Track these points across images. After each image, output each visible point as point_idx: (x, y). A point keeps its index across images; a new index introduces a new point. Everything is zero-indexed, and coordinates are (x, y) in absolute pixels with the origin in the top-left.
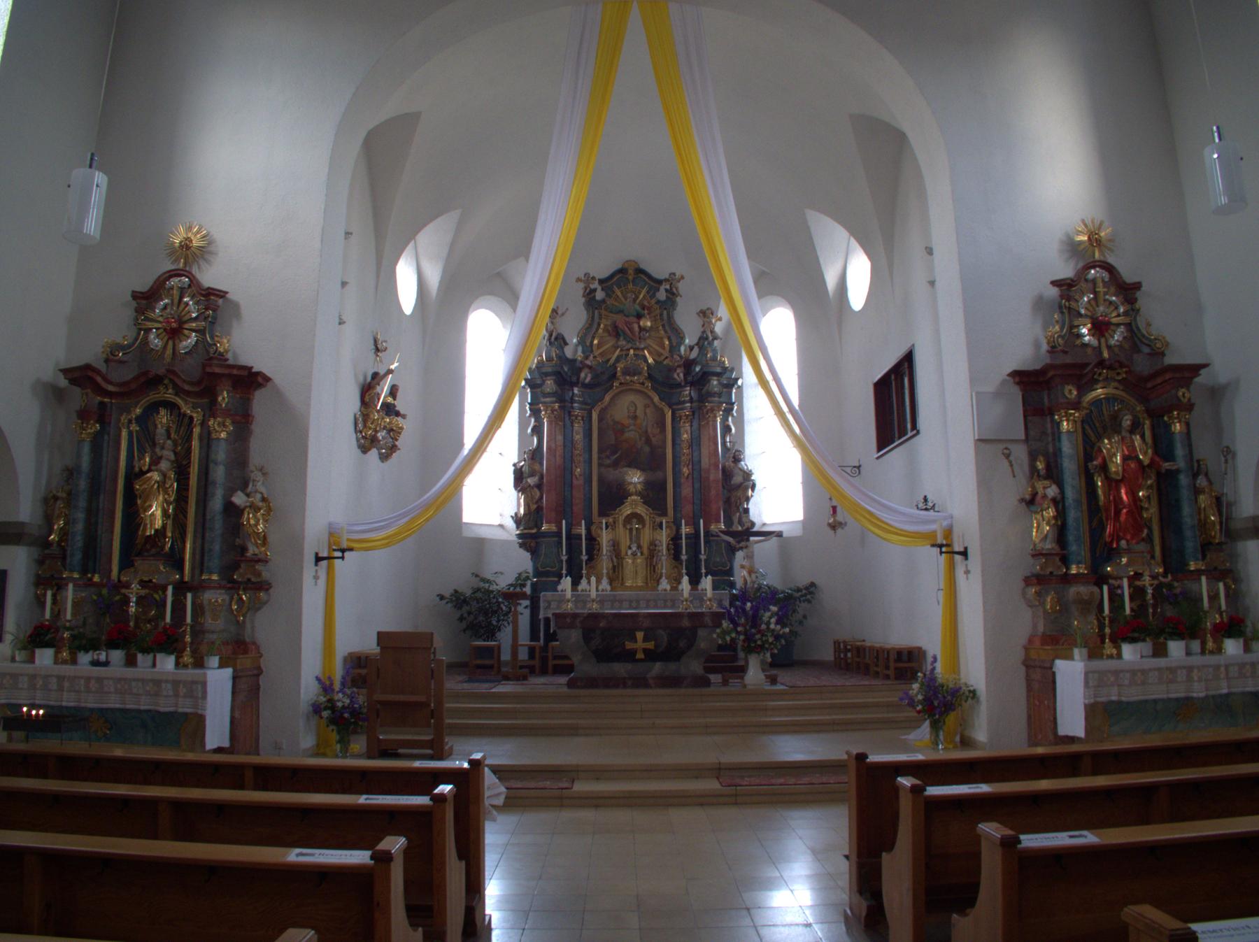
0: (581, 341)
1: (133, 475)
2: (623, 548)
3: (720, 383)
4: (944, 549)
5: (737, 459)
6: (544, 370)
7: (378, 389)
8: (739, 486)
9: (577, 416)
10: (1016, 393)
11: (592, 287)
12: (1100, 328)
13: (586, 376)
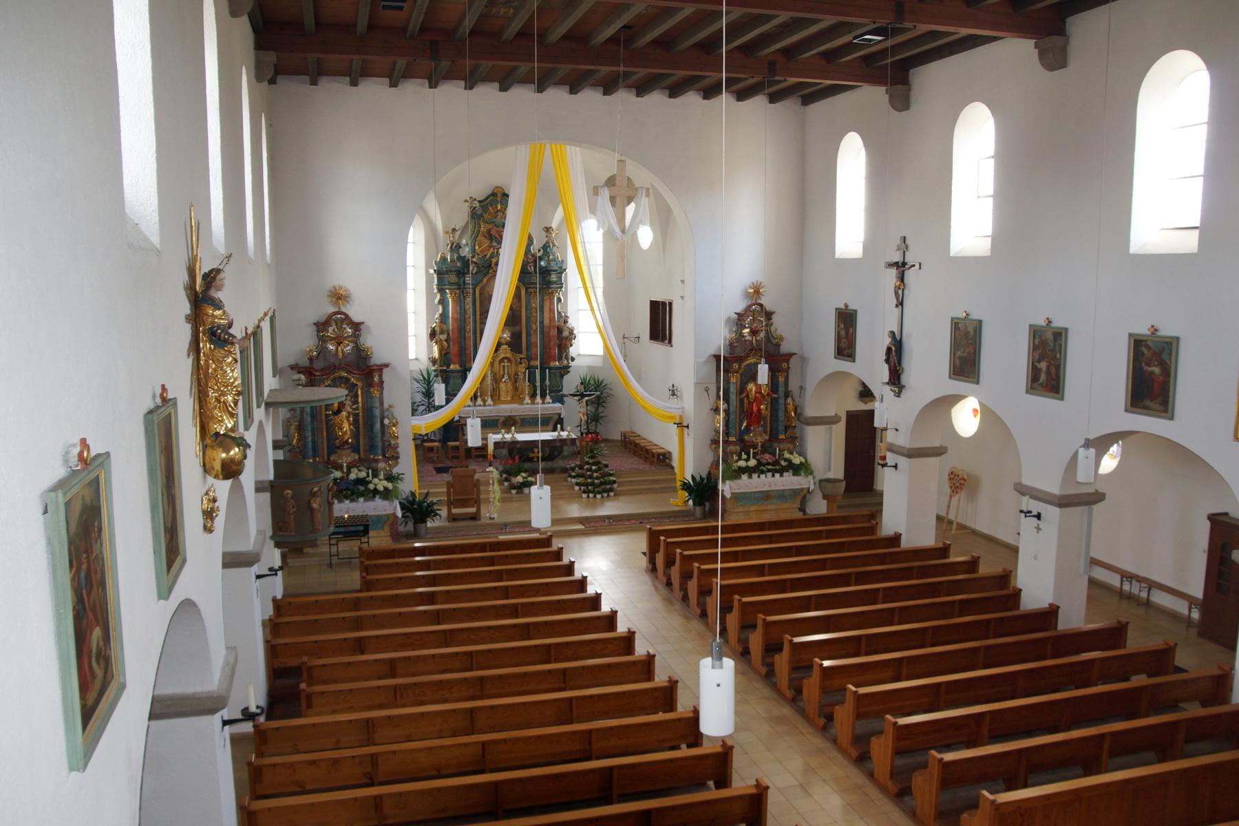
5: (566, 322)
12: (754, 332)
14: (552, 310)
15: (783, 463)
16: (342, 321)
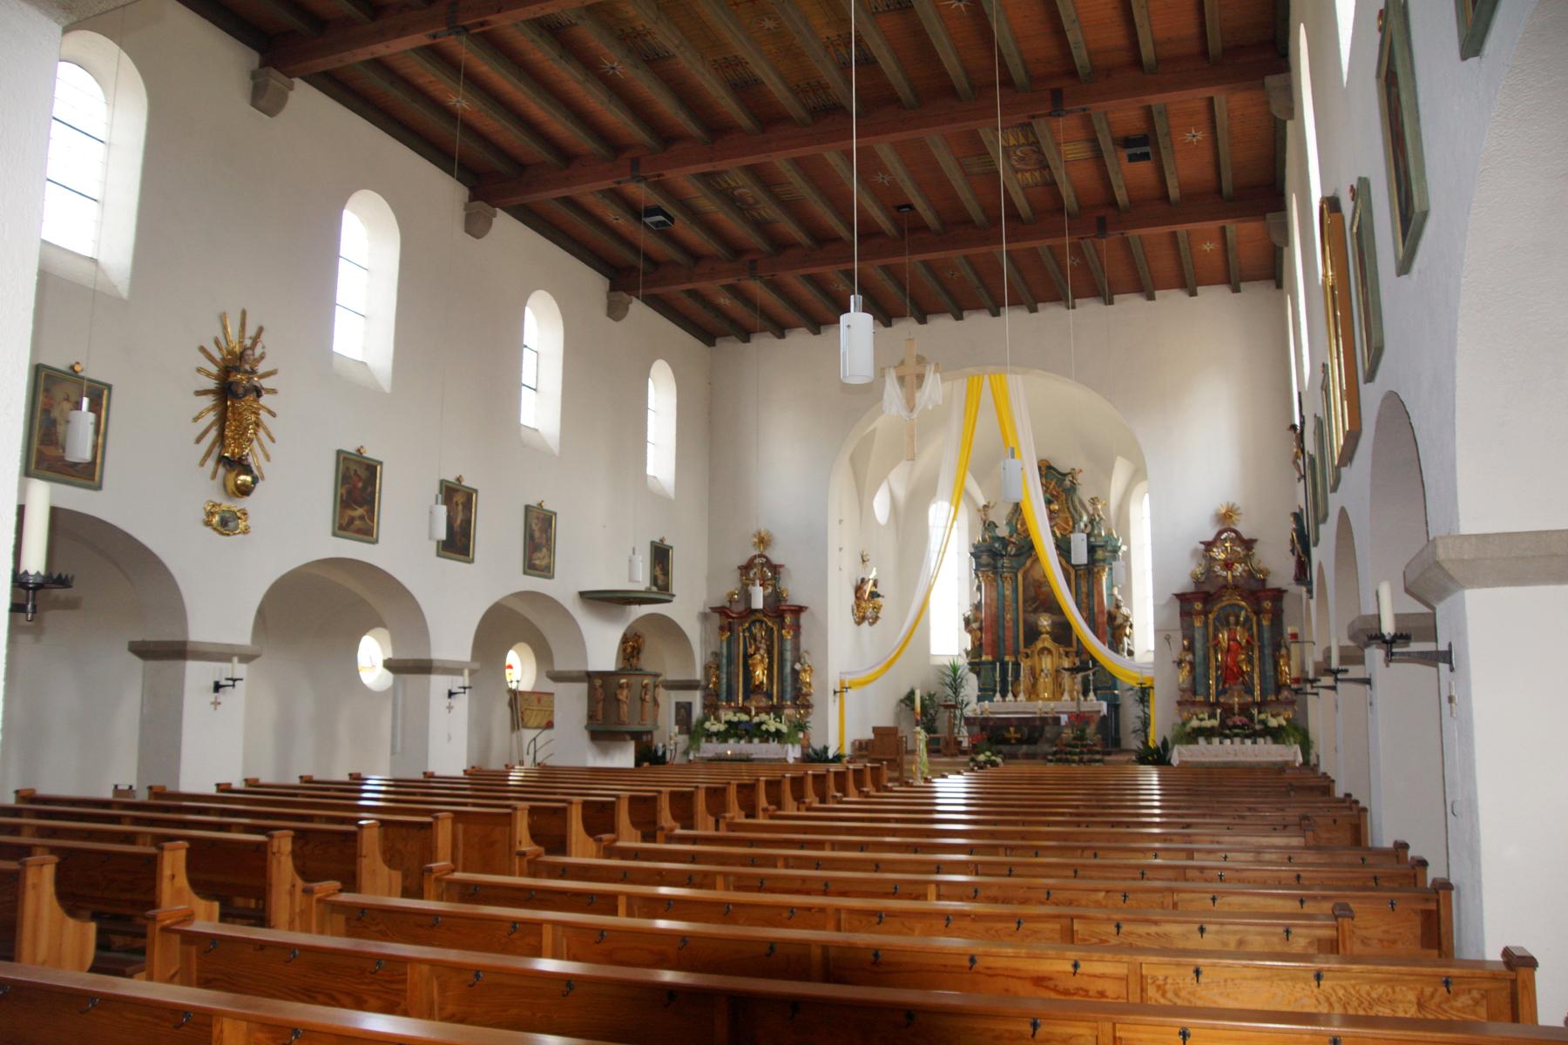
1: (747, 657)
5: (1118, 607)
10: (1177, 604)
13: (1012, 550)
15: (1258, 727)
16: (762, 565)
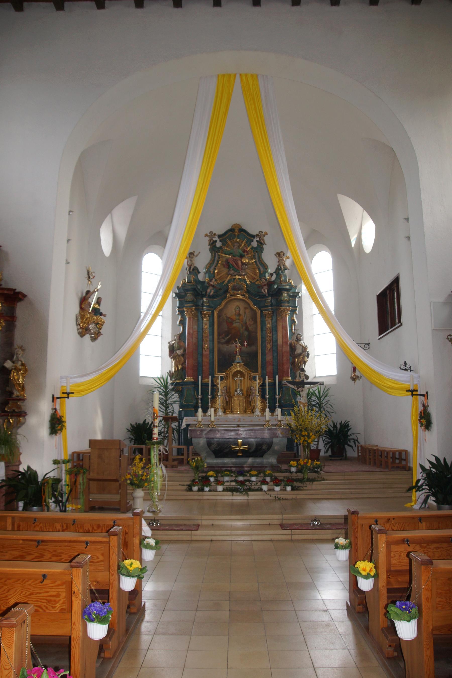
0: (208, 271)
2: (232, 390)
3: (288, 295)
4: (414, 393)
5: (298, 339)
6: (186, 288)
7: (90, 300)
8: (300, 355)
9: (205, 315)
11: (214, 239)
14: (285, 328)
